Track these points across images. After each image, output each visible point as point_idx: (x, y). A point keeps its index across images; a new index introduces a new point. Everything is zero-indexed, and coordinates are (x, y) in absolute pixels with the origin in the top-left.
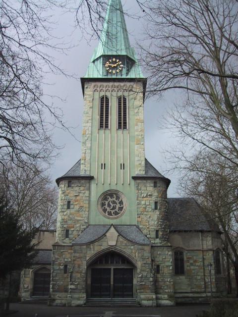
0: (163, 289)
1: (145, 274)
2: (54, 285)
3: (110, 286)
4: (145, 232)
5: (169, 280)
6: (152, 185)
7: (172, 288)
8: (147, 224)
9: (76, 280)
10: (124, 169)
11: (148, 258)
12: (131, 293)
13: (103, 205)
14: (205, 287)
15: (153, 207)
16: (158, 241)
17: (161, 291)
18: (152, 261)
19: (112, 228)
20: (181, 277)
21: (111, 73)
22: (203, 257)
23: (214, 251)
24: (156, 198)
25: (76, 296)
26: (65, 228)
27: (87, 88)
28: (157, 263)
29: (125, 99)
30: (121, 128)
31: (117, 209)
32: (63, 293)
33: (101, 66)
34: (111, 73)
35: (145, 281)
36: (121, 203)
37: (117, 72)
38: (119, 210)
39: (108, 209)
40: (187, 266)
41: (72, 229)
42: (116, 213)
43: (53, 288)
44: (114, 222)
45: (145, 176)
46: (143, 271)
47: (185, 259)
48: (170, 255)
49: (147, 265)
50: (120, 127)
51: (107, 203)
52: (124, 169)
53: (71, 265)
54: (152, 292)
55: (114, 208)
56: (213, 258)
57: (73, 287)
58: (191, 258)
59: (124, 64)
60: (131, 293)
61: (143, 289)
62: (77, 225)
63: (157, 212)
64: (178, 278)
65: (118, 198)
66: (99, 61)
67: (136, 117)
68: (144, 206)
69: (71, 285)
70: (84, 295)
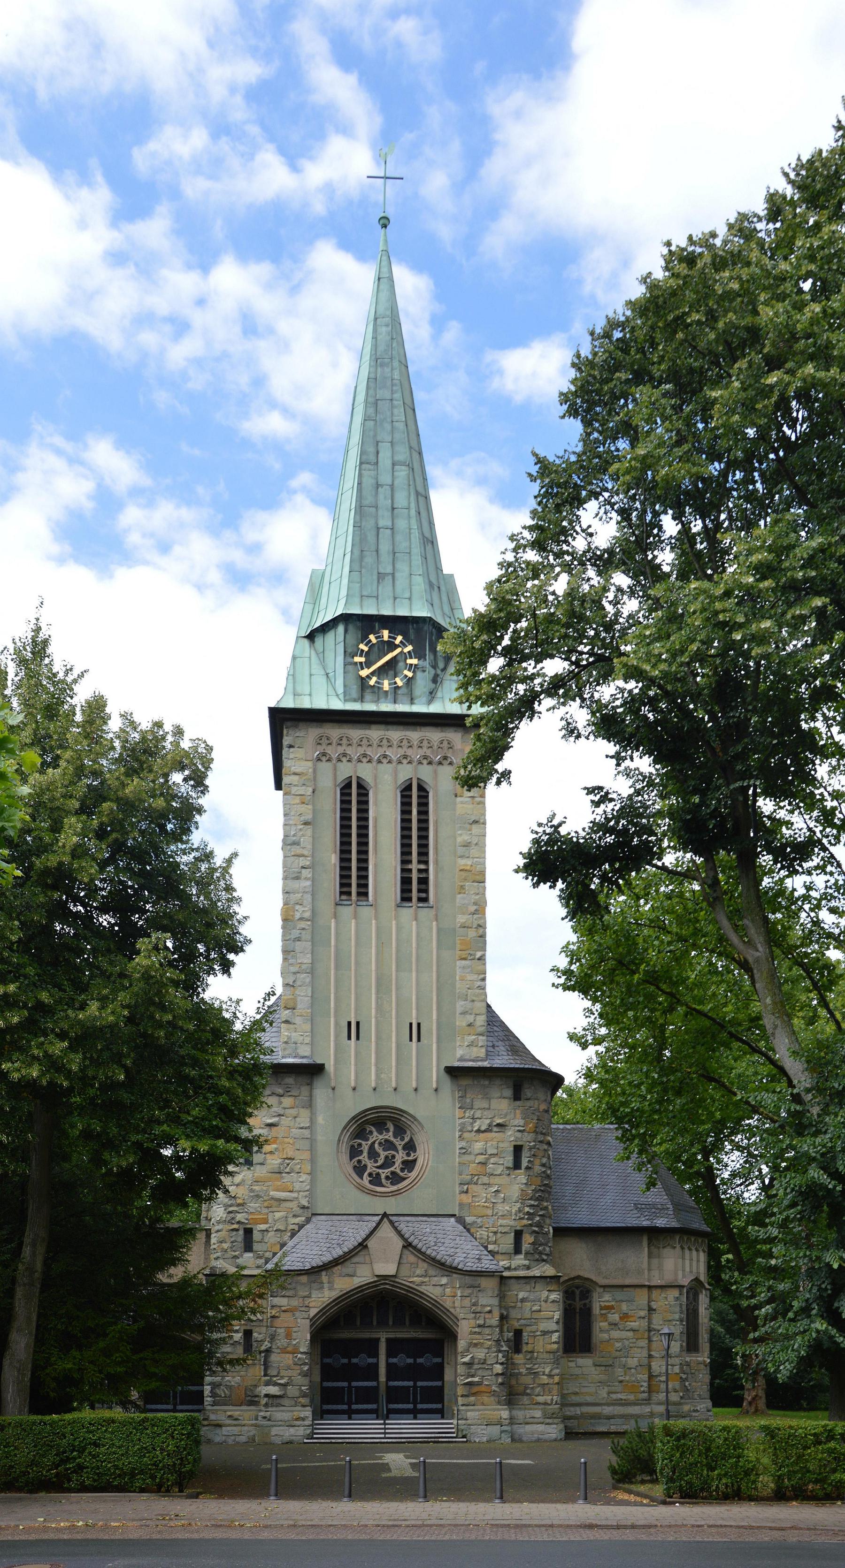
0: (528, 1394)
1: (480, 1354)
2: (214, 1386)
3: (377, 1388)
4: (482, 1233)
5: (547, 1371)
6: (509, 1093)
7: (555, 1392)
8: (490, 1212)
9: (283, 1373)
10: (419, 1040)
11: (490, 1312)
12: (439, 1406)
13: (354, 1152)
14: (650, 1391)
15: (509, 1160)
16: (520, 1260)
17: (525, 1400)
18: (503, 1318)
19: (386, 1224)
20: (581, 1361)
21: (377, 690)
22: (649, 1306)
23: (681, 1287)
24: (519, 1135)
25: (280, 1415)
26: (239, 1222)
27: (291, 746)
28: (516, 1325)
29: (423, 792)
30: (410, 899)
31: (397, 1167)
32: (244, 1408)
33: (340, 659)
34: (377, 690)
35: (480, 1372)
36: (410, 1147)
37: (397, 688)
38: (402, 1170)
39: (371, 1166)
40: (601, 1331)
41: (263, 1227)
42: (395, 1179)
43: (213, 1394)
44: (391, 1206)
45: (486, 1064)
46: (476, 1345)
47: (596, 1310)
48: (553, 1301)
49: (487, 1331)
50: (406, 897)
51: (365, 1147)
52: (419, 1040)
53: (264, 1330)
54: (499, 1403)
55: (388, 1162)
56: (677, 1309)
57: (273, 1390)
58: (612, 1307)
59: (420, 656)
60: (439, 1406)
61: (474, 1394)
62: (278, 1215)
63: (521, 1177)
64: (572, 1364)
65: (400, 1131)
66: (330, 636)
67: (462, 862)
68: (481, 1158)
69: (267, 1384)
70: (308, 1413)
